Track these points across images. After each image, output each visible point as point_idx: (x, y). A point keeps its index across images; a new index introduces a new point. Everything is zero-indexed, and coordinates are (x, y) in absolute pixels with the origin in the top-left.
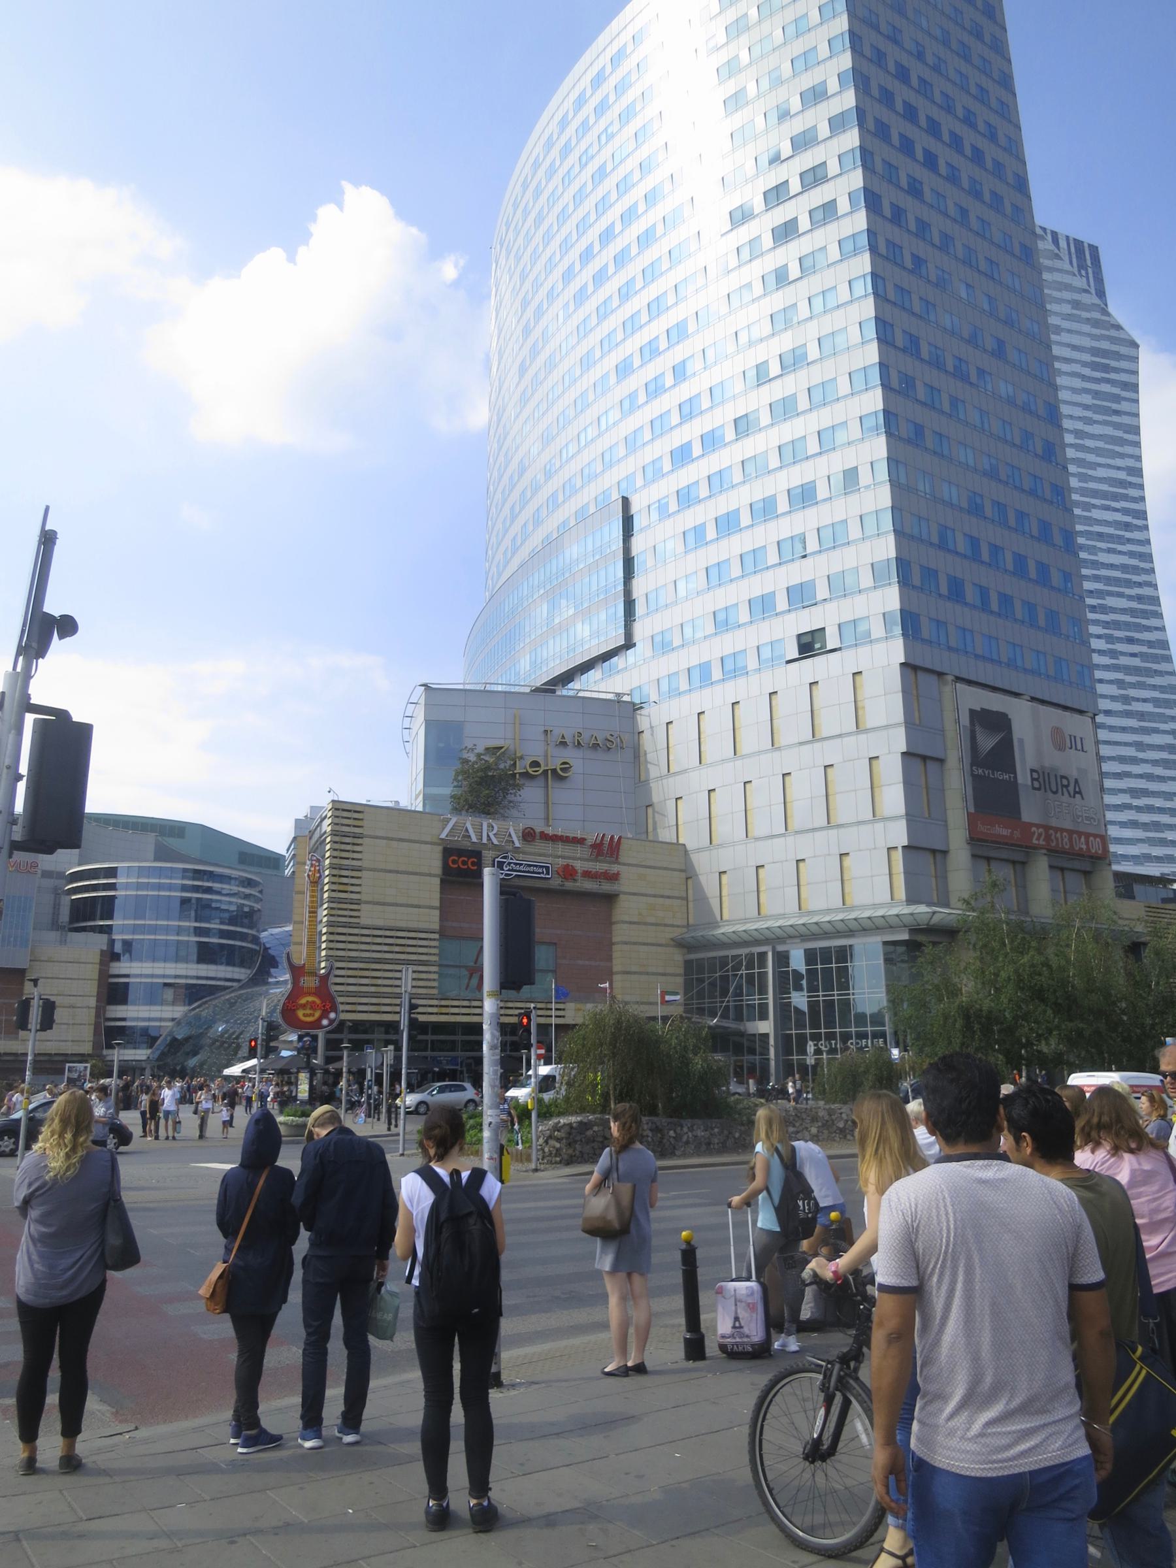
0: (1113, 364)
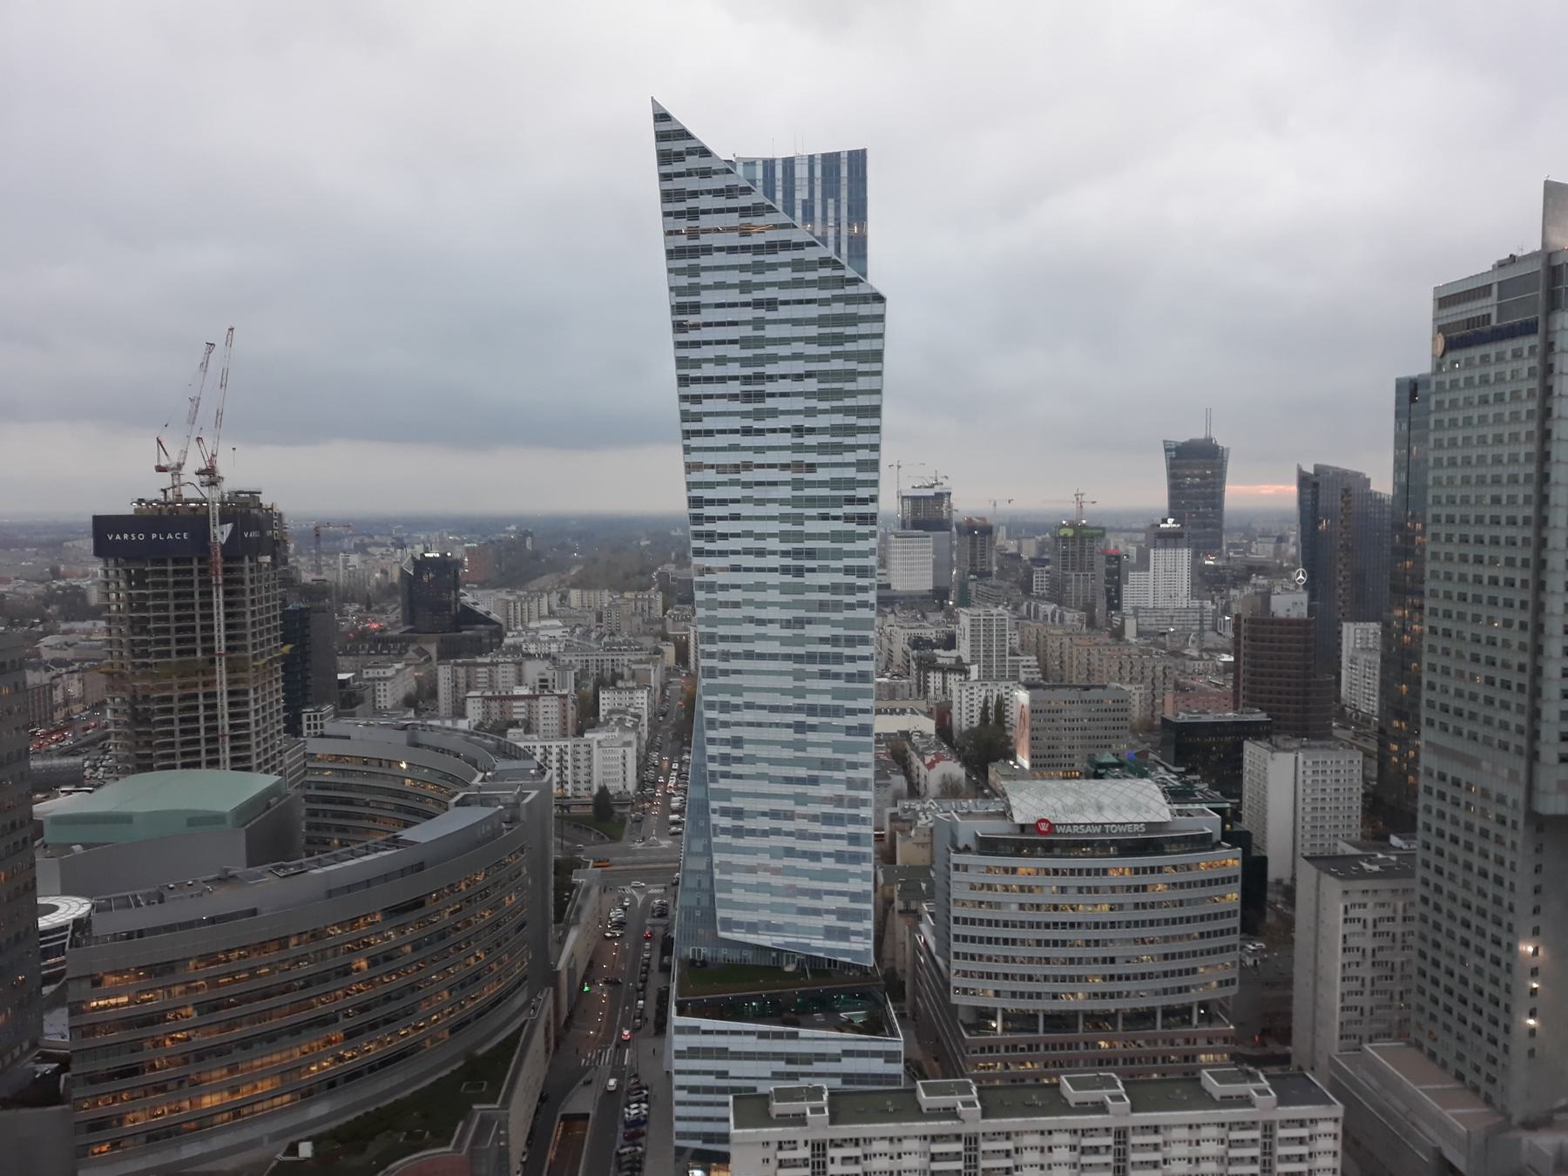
0: (849, 331)
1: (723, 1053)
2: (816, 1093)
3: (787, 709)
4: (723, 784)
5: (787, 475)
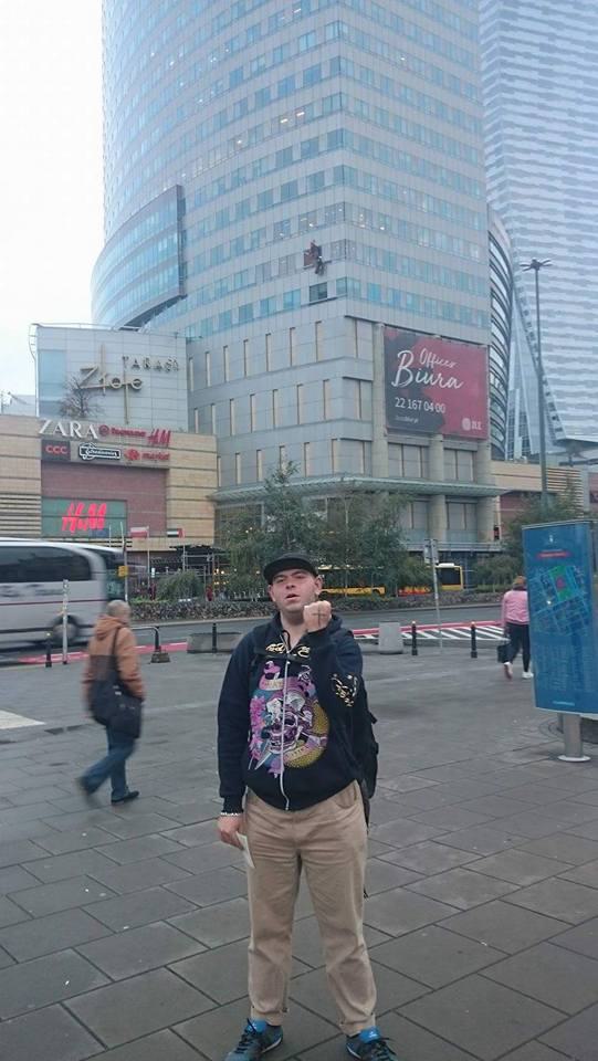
5: (565, 141)
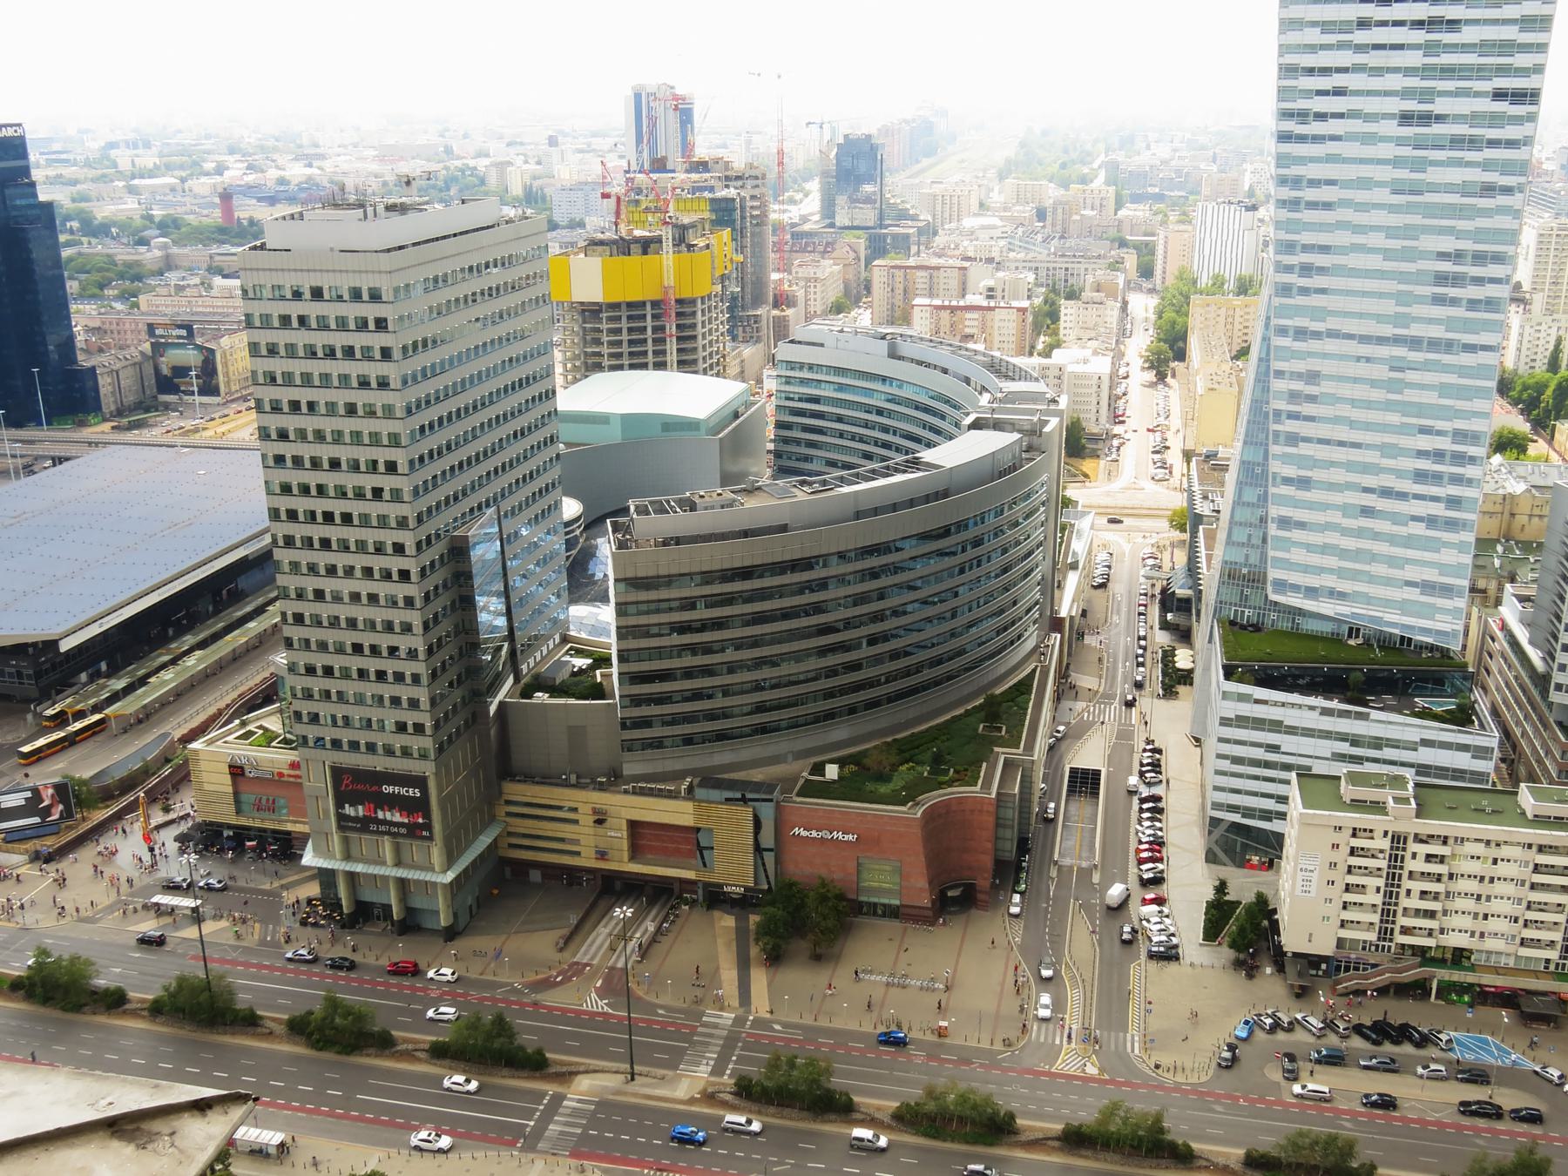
1: (1276, 726)
2: (1398, 781)
3: (1381, 340)
4: (1290, 426)
5: (1419, 36)
